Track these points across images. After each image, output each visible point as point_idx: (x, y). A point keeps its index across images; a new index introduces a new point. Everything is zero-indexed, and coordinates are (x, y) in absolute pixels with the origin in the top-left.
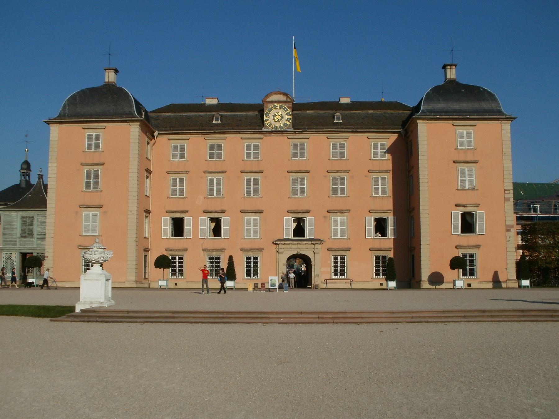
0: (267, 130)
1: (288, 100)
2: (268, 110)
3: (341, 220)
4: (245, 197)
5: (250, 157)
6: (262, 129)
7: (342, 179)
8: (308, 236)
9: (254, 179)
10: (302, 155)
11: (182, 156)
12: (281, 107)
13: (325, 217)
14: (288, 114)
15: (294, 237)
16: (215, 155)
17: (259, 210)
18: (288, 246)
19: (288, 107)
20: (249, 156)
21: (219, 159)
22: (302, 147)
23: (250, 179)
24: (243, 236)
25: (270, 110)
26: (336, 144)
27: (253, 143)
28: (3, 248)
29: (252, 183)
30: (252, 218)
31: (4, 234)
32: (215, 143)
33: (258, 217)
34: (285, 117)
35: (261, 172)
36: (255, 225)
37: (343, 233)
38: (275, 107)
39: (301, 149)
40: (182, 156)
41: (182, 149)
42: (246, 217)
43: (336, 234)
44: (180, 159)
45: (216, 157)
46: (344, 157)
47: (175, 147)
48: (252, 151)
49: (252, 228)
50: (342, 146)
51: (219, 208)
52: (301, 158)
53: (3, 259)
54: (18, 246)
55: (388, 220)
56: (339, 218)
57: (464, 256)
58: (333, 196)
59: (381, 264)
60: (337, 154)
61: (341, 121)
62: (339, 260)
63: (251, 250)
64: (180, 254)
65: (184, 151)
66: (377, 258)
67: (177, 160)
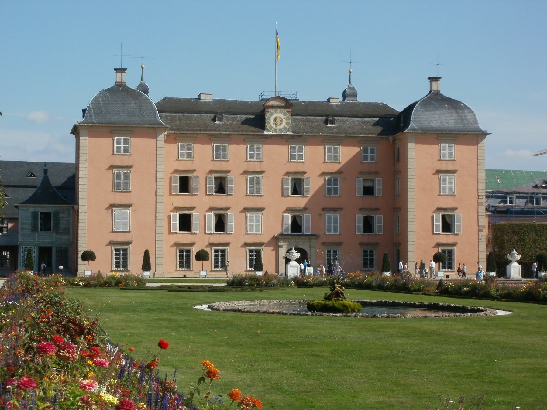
0: (269, 133)
3: (334, 217)
5: (252, 158)
6: (263, 132)
7: (336, 180)
8: (305, 231)
9: (257, 179)
11: (189, 155)
12: (281, 112)
13: (320, 214)
14: (287, 119)
15: (292, 232)
19: (287, 112)
20: (251, 157)
21: (224, 159)
25: (272, 114)
26: (330, 148)
28: (22, 243)
29: (255, 182)
31: (22, 229)
33: (259, 214)
34: (284, 121)
37: (335, 230)
43: (329, 230)
44: (187, 157)
46: (337, 159)
48: (255, 153)
52: (299, 160)
53: (22, 252)
54: (37, 240)
55: (376, 218)
56: (332, 216)
57: (444, 251)
58: (328, 195)
59: (368, 257)
60: (331, 157)
62: (332, 253)
64: (188, 248)
65: (191, 150)
66: (365, 252)
67: (184, 159)
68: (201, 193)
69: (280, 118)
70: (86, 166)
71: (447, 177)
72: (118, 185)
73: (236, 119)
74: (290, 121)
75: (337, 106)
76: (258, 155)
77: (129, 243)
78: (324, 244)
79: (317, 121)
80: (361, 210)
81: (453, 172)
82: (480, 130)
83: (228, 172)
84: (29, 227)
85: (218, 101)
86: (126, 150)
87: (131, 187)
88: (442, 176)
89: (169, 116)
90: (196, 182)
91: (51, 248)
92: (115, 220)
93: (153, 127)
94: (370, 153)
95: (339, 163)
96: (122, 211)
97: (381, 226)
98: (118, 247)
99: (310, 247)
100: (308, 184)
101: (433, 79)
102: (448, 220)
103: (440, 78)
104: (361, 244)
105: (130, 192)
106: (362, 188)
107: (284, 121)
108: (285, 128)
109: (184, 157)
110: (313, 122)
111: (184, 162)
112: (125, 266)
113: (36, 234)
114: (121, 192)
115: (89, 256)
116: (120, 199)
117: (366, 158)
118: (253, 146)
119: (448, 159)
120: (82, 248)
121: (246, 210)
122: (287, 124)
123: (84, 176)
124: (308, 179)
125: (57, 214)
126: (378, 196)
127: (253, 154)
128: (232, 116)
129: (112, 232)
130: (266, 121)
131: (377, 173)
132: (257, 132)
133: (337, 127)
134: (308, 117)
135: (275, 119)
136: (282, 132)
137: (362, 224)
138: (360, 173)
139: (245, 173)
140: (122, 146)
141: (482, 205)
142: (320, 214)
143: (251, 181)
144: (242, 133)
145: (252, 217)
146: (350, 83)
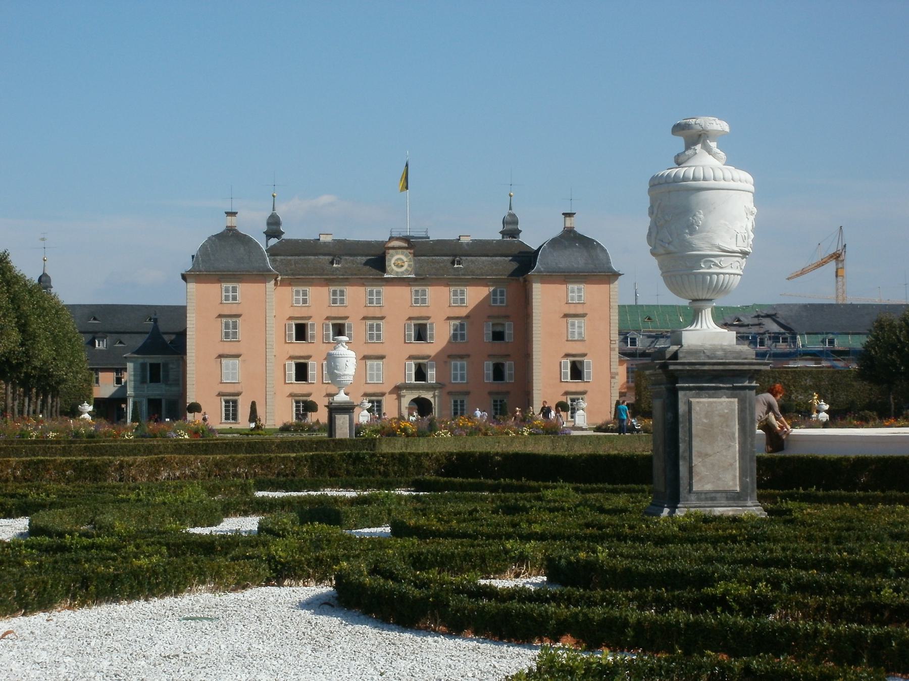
0: (389, 276)
2: (390, 256)
3: (461, 364)
4: (368, 343)
5: (372, 303)
9: (377, 325)
10: (424, 301)
11: (305, 301)
12: (402, 254)
13: (445, 362)
20: (371, 302)
23: (373, 325)
25: (392, 256)
26: (457, 291)
27: (375, 289)
29: (375, 329)
32: (338, 288)
36: (378, 369)
37: (462, 378)
38: (397, 254)
39: (422, 296)
41: (305, 294)
42: (369, 362)
43: (455, 379)
47: (298, 293)
48: (375, 297)
50: (462, 293)
61: (461, 266)
62: (459, 403)
65: (306, 296)
66: (495, 401)
68: (318, 340)
70: (194, 315)
71: (576, 321)
72: (227, 335)
73: (356, 262)
74: (412, 263)
75: (468, 244)
76: (378, 301)
77: (238, 394)
78: (450, 393)
79: (443, 261)
80: (490, 356)
81: (583, 316)
82: (610, 270)
83: (346, 318)
85: (339, 241)
86: (234, 298)
87: (240, 336)
88: (570, 320)
89: (284, 259)
90: (312, 330)
92: (224, 371)
93: (262, 275)
95: (466, 306)
96: (230, 361)
97: (511, 374)
98: (228, 398)
100: (432, 329)
101: (568, 215)
102: (579, 366)
103: (575, 214)
104: (490, 393)
105: (239, 341)
106: (491, 335)
107: (406, 264)
108: (407, 270)
110: (438, 263)
111: (299, 308)
112: (235, 418)
113: (146, 386)
114: (231, 341)
115: (195, 408)
116: (229, 348)
117: (495, 301)
118: (373, 291)
119: (577, 302)
120: (191, 399)
122: (409, 266)
123: (192, 326)
124: (432, 324)
125: (166, 365)
126: (508, 342)
128: (352, 258)
129: (221, 383)
130: (387, 264)
131: (507, 317)
132: (377, 275)
133: (464, 268)
134: (434, 258)
135: (397, 260)
136: (404, 274)
137: (491, 372)
138: (489, 317)
139: (365, 318)
140: (231, 294)
142: (445, 362)
144: (361, 277)
145: (372, 366)
146: (510, 209)
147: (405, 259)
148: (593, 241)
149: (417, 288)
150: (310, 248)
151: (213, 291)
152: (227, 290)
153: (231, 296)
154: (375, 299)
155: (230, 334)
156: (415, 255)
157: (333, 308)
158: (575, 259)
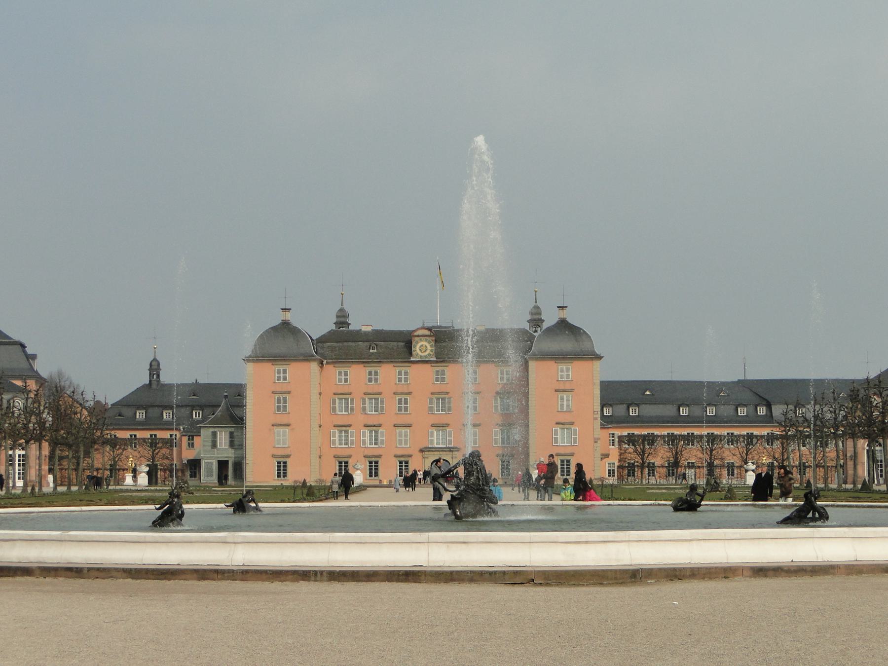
1: (432, 334)
5: (401, 381)
6: (410, 359)
10: (443, 379)
11: (346, 380)
12: (426, 340)
14: (431, 346)
16: (373, 379)
17: (409, 424)
18: (432, 453)
19: (432, 340)
20: (400, 380)
22: (443, 373)
23: (401, 399)
24: (396, 445)
25: (417, 342)
27: (403, 370)
29: (403, 402)
30: (403, 431)
31: (204, 446)
32: (373, 369)
35: (410, 393)
36: (406, 436)
38: (421, 340)
39: (443, 375)
40: (346, 380)
41: (346, 375)
45: (373, 381)
47: (340, 374)
48: (403, 377)
49: (403, 438)
51: (376, 423)
63: (402, 456)
64: (346, 459)
65: (347, 376)
69: (426, 346)
72: (279, 408)
74: (434, 348)
77: (288, 456)
81: (572, 390)
84: (210, 444)
86: (285, 378)
88: (560, 395)
91: (228, 461)
94: (506, 375)
96: (281, 429)
99: (452, 458)
101: (562, 308)
108: (429, 355)
109: (342, 382)
119: (566, 380)
121: (395, 426)
122: (431, 351)
124: (450, 398)
127: (401, 378)
135: (422, 345)
140: (282, 375)
141: (597, 419)
143: (400, 400)
146: (536, 302)
147: (429, 347)
148: (580, 329)
149: (438, 369)
150: (357, 336)
151: (269, 370)
152: (279, 372)
153: (282, 377)
154: (403, 379)
155: (282, 406)
156: (436, 341)
157: (369, 386)
158: (565, 344)
